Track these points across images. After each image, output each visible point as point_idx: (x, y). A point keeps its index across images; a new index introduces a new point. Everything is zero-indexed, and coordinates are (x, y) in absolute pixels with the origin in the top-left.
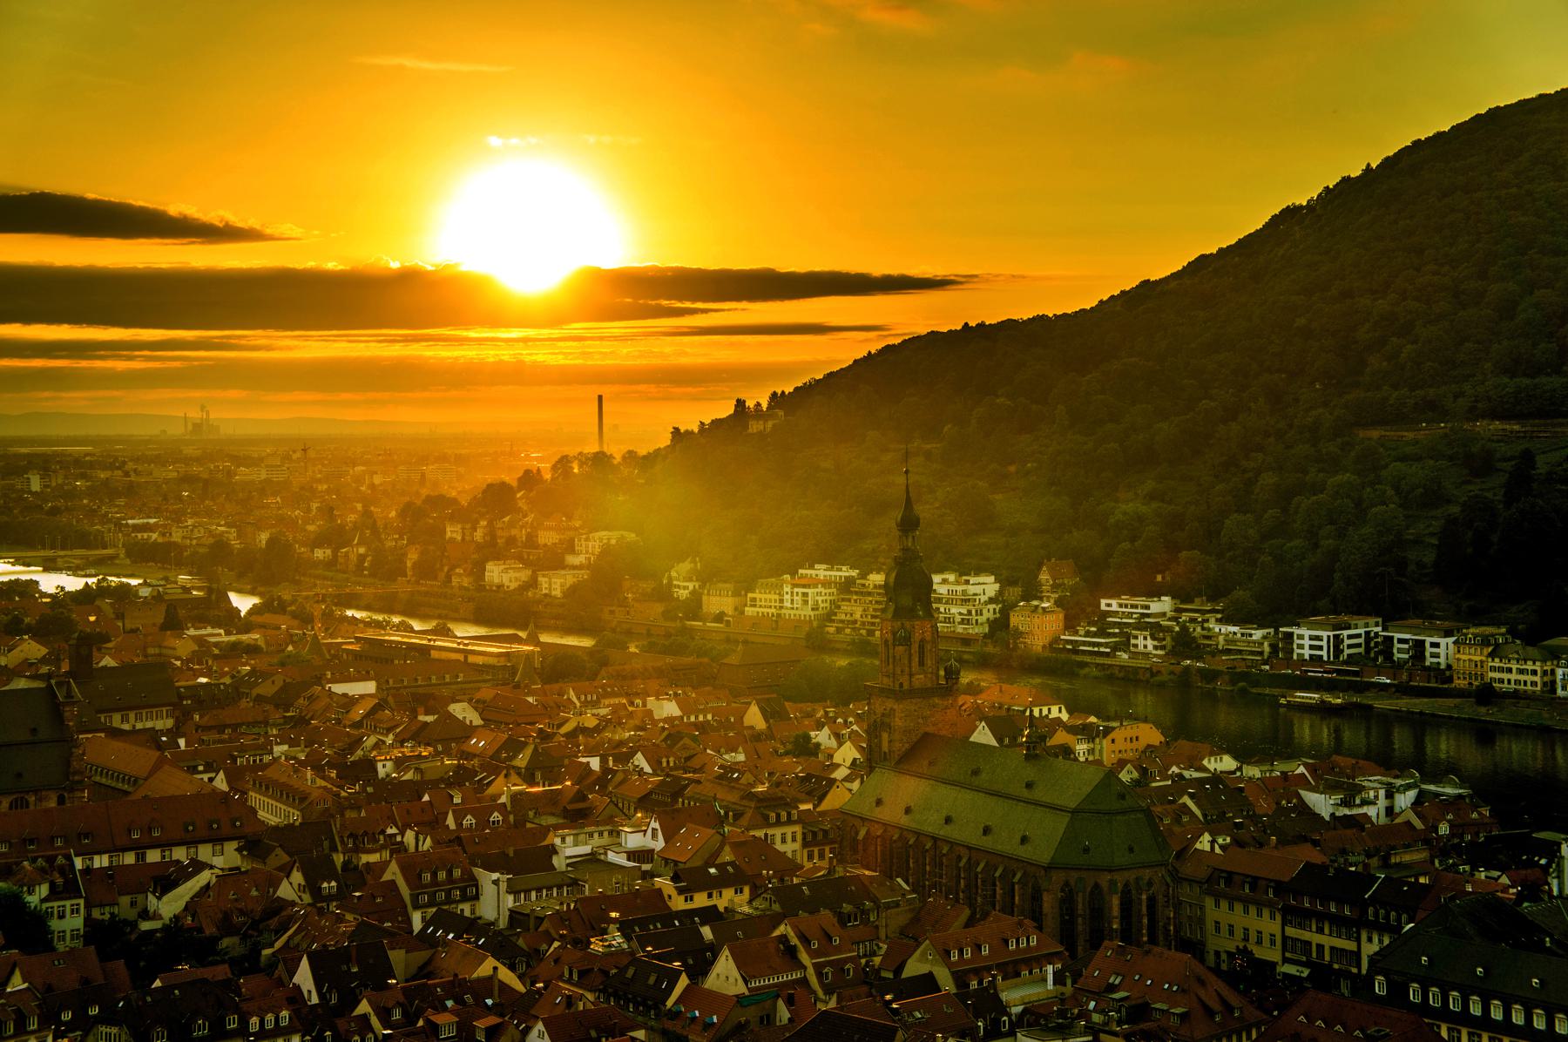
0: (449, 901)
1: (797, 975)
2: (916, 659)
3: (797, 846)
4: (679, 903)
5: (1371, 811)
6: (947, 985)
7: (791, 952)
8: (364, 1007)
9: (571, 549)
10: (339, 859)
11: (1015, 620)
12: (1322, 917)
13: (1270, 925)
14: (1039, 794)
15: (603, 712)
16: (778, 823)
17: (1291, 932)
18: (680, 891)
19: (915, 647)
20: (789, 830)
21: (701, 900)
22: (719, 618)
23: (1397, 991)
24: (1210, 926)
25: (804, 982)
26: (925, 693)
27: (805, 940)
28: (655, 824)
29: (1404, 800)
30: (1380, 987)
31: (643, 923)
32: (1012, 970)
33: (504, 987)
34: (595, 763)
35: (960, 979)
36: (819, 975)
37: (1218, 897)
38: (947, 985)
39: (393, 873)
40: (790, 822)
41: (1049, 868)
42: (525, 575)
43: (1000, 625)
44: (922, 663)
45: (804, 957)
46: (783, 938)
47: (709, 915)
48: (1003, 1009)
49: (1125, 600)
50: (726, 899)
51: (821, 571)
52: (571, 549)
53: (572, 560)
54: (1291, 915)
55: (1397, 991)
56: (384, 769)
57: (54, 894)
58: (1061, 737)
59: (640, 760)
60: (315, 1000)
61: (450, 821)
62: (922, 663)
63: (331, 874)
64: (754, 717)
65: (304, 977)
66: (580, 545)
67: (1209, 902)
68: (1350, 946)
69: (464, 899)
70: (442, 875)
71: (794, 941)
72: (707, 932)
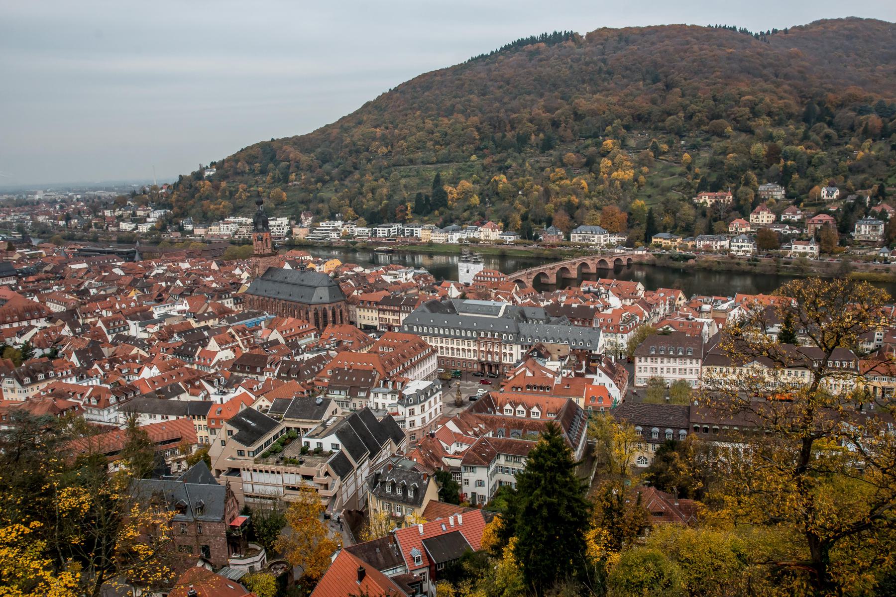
4: (195, 325)
5: (401, 280)
6: (282, 341)
7: (233, 336)
8: (96, 366)
9: (148, 216)
10: (81, 321)
11: (295, 230)
12: (389, 311)
13: (374, 314)
14: (305, 283)
15: (165, 268)
16: (225, 298)
17: (381, 316)
18: (196, 322)
20: (229, 300)
21: (203, 324)
22: (200, 236)
23: (411, 329)
24: (358, 317)
25: (238, 346)
26: (269, 255)
27: (237, 332)
28: (185, 302)
29: (410, 276)
30: (406, 329)
31: (185, 332)
32: (301, 335)
33: (141, 356)
34: (164, 284)
35: (286, 339)
36: (243, 343)
38: (282, 341)
39: (100, 324)
42: (133, 226)
43: (290, 233)
45: (237, 338)
46: (230, 333)
47: (206, 328)
48: (299, 347)
50: (210, 323)
51: (232, 219)
52: (148, 216)
53: (148, 220)
54: (380, 310)
55: (411, 329)
56: (93, 291)
58: (311, 265)
59: (179, 282)
60: (79, 365)
61: (117, 306)
63: (78, 325)
64: (214, 266)
65: (74, 359)
66: (151, 215)
67: (358, 310)
68: (397, 318)
69: (125, 330)
70: (117, 323)
71: (234, 333)
72: (206, 333)
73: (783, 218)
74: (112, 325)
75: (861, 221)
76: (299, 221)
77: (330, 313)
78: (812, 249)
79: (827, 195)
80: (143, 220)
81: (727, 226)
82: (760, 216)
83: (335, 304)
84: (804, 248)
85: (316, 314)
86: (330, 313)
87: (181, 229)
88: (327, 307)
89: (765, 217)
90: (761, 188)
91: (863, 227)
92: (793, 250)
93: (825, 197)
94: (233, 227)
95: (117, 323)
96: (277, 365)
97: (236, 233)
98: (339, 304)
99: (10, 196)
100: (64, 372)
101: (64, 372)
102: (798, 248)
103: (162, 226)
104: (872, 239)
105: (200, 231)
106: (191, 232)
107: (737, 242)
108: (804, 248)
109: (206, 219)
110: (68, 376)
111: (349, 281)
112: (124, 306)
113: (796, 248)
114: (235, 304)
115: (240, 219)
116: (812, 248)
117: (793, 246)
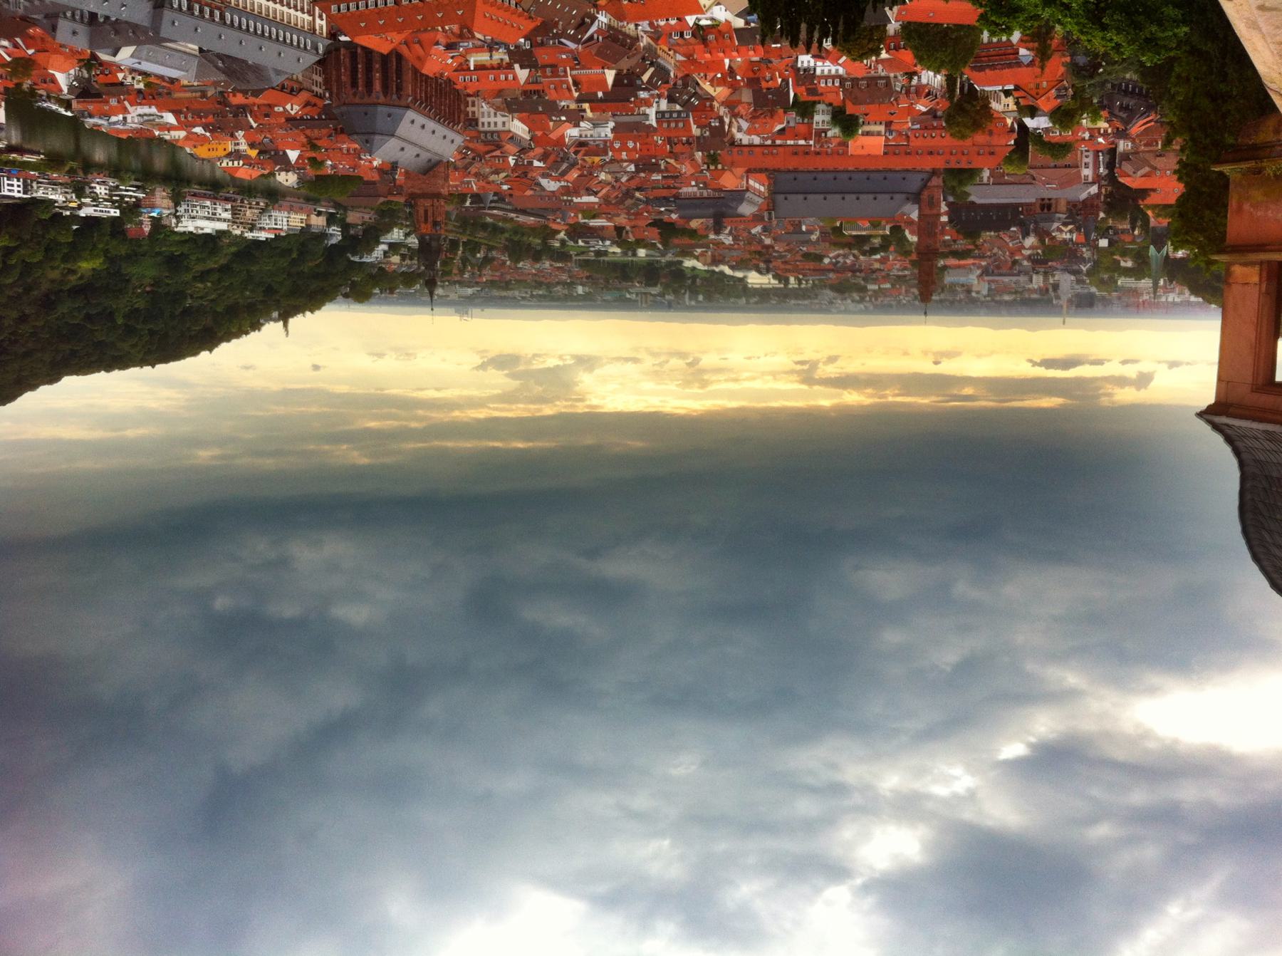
0: (671, 112)
1: (574, 72)
2: (430, 214)
3: (481, 120)
7: (576, 83)
9: (385, 252)
16: (492, 133)
19: (430, 220)
20: (486, 128)
22: (319, 214)
26: (424, 196)
27: (569, 89)
37: (297, 81)
40: (486, 133)
41: (408, 107)
44: (426, 212)
49: (104, 215)
51: (263, 236)
52: (385, 252)
53: (385, 247)
57: (825, 131)
62: (426, 212)
69: (663, 113)
70: (673, 125)
74: (681, 125)
76: (156, 222)
77: (377, 86)
80: (394, 247)
83: (366, 100)
85: (399, 89)
86: (377, 86)
87: (345, 227)
88: (382, 99)
94: (266, 222)
95: (673, 125)
96: (591, 38)
97: (263, 211)
98: (357, 100)
99: (504, 294)
100: (830, 84)
101: (830, 84)
103: (371, 236)
105: (318, 222)
106: (331, 219)
109: (306, 238)
110: (826, 78)
111: (255, 125)
112: (631, 144)
114: (476, 121)
115: (249, 235)
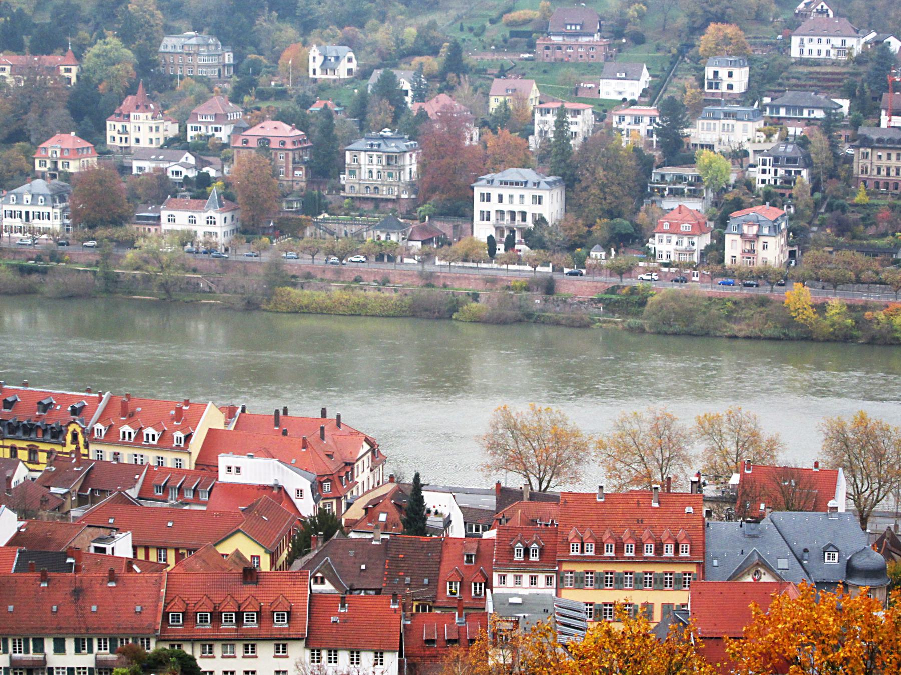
73: (191, 134)
75: (361, 144)
78: (210, 224)
79: (325, 68)
81: (29, 157)
82: (130, 127)
84: (193, 221)
89: (145, 128)
90: (169, 43)
91: (363, 158)
92: (165, 226)
93: (319, 75)
102: (177, 219)
104: (384, 193)
107: (19, 201)
108: (193, 221)
113: (171, 220)
116: (211, 221)
117: (164, 215)
